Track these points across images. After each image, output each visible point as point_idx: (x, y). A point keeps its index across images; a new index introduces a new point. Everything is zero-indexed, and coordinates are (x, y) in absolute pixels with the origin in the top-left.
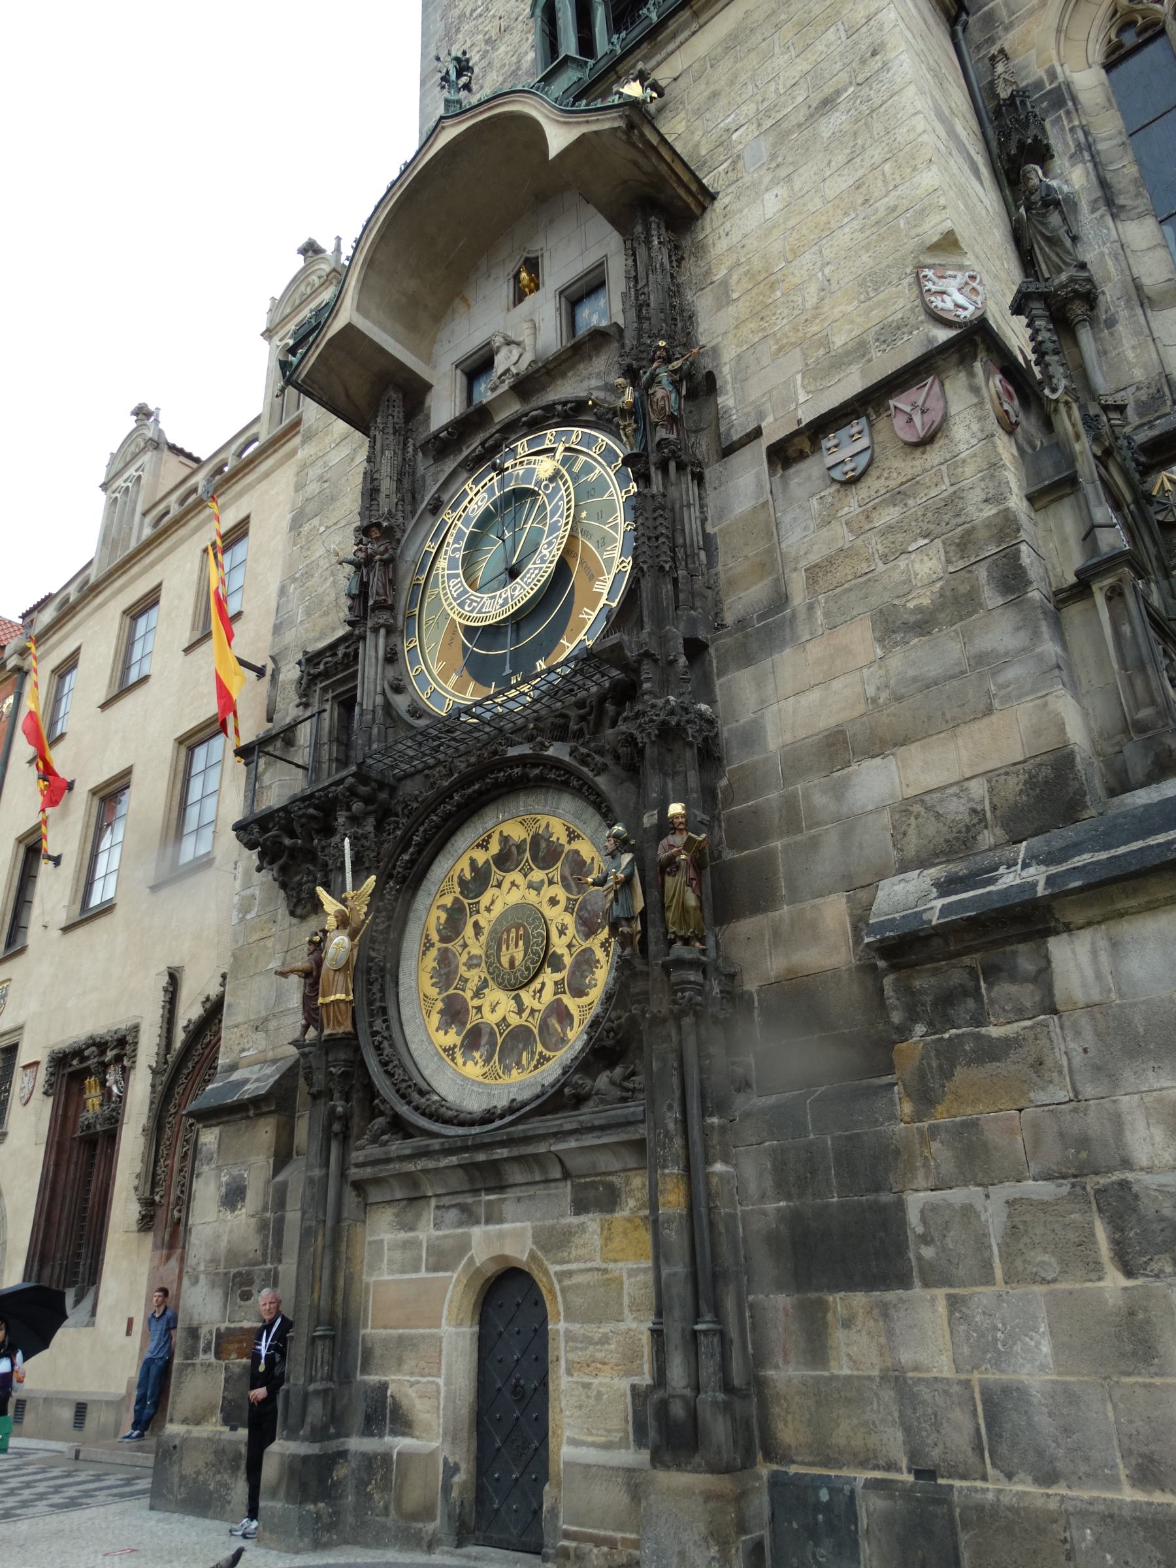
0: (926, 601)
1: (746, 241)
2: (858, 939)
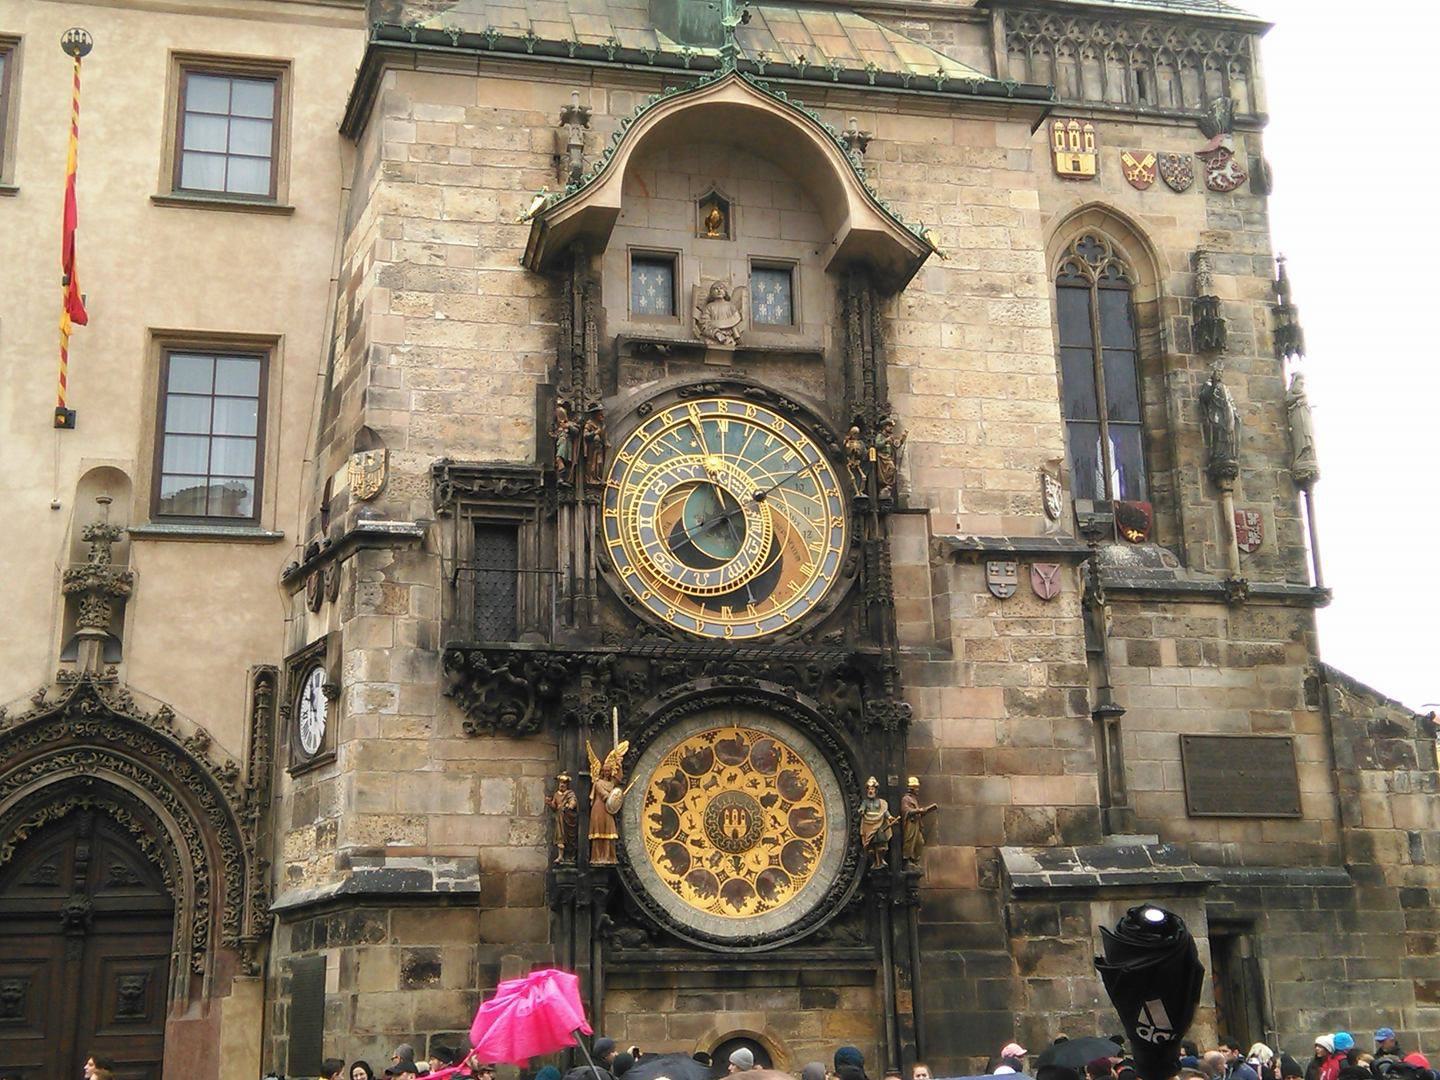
0: (1035, 697)
2: (981, 874)
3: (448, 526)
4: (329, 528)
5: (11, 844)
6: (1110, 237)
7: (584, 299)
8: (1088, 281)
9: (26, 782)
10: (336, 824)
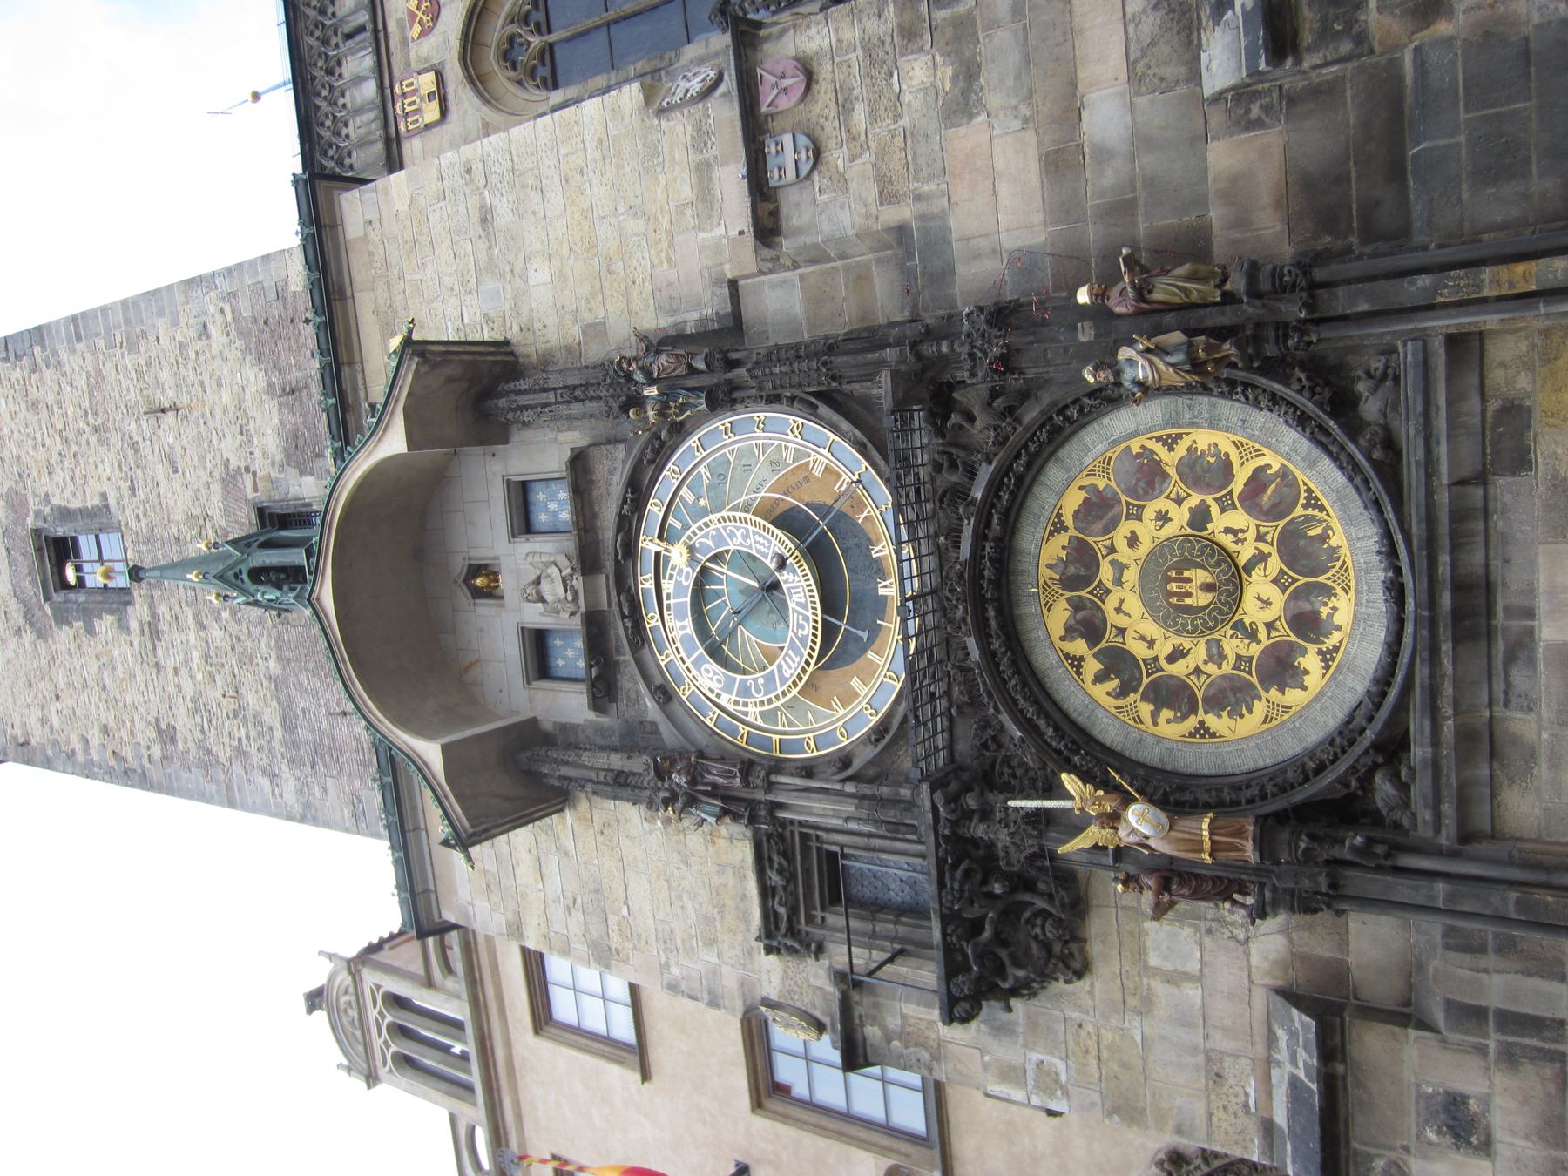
0: (950, 70)
1: (559, 305)
2: (1258, 124)
6: (496, 31)
7: (566, 763)
8: (542, 52)
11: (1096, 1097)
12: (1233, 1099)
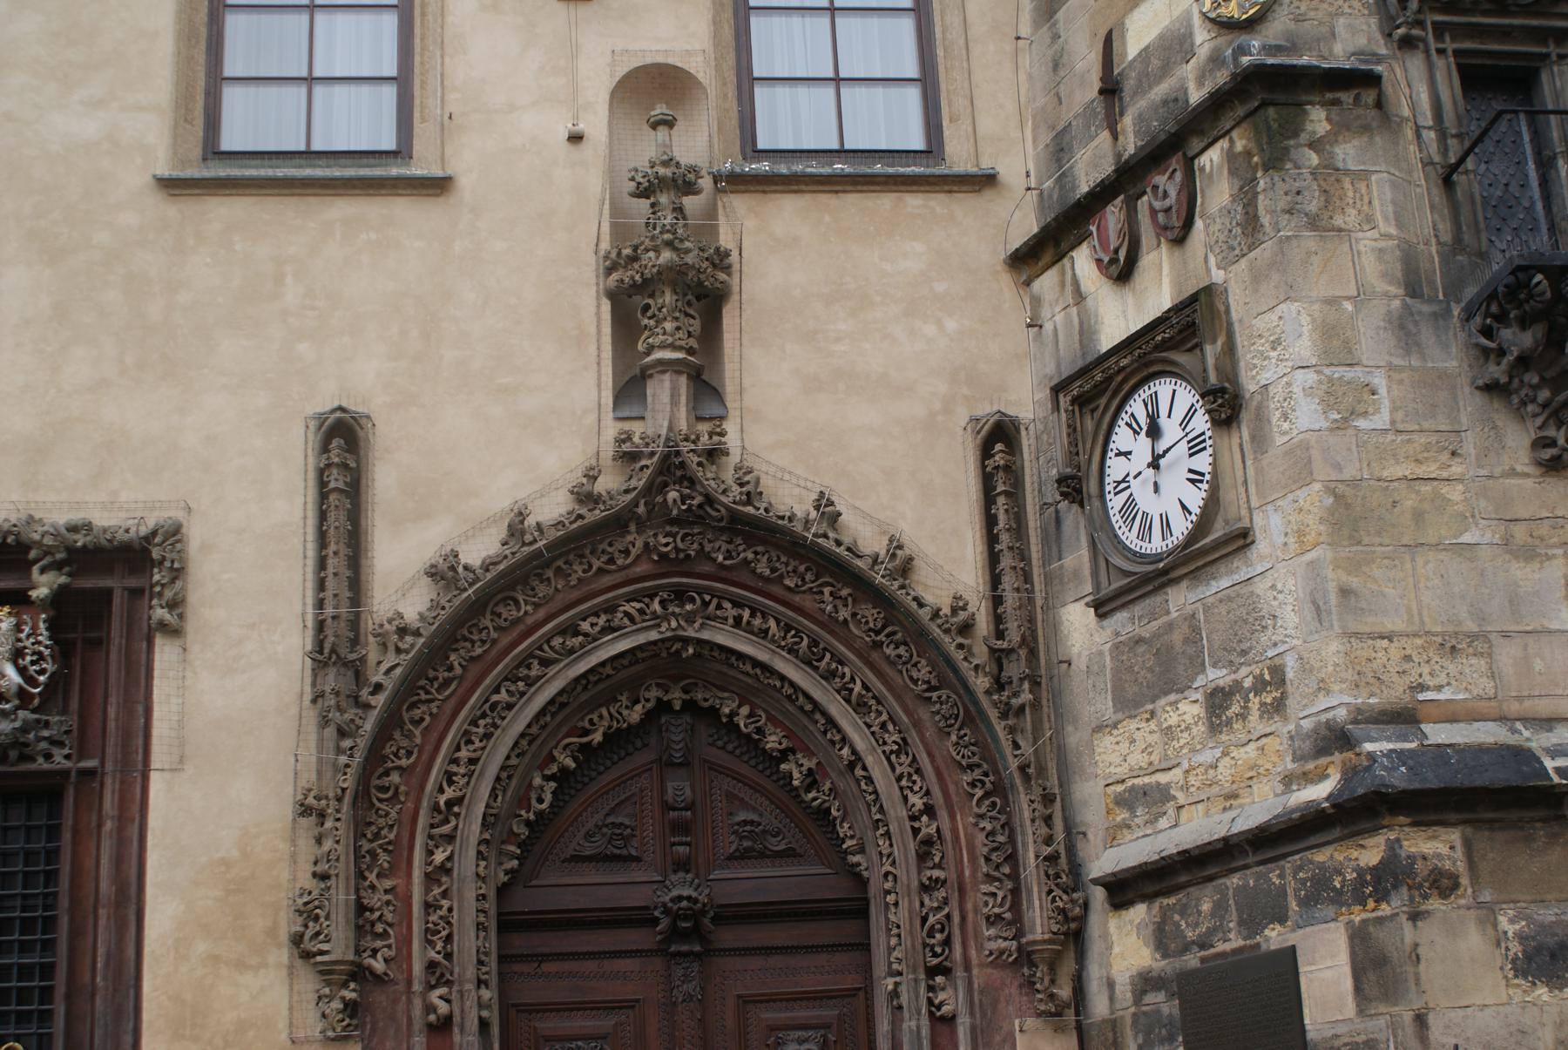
3: (1415, 64)
4: (1128, 122)
5: (547, 778)
9: (572, 651)
10: (1278, 673)
11: (1350, 472)
12: (1426, 670)
